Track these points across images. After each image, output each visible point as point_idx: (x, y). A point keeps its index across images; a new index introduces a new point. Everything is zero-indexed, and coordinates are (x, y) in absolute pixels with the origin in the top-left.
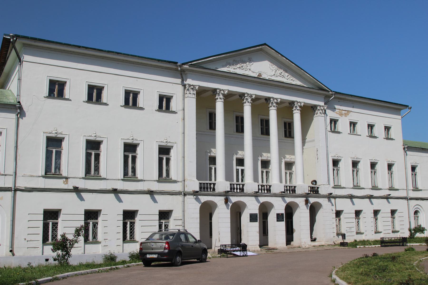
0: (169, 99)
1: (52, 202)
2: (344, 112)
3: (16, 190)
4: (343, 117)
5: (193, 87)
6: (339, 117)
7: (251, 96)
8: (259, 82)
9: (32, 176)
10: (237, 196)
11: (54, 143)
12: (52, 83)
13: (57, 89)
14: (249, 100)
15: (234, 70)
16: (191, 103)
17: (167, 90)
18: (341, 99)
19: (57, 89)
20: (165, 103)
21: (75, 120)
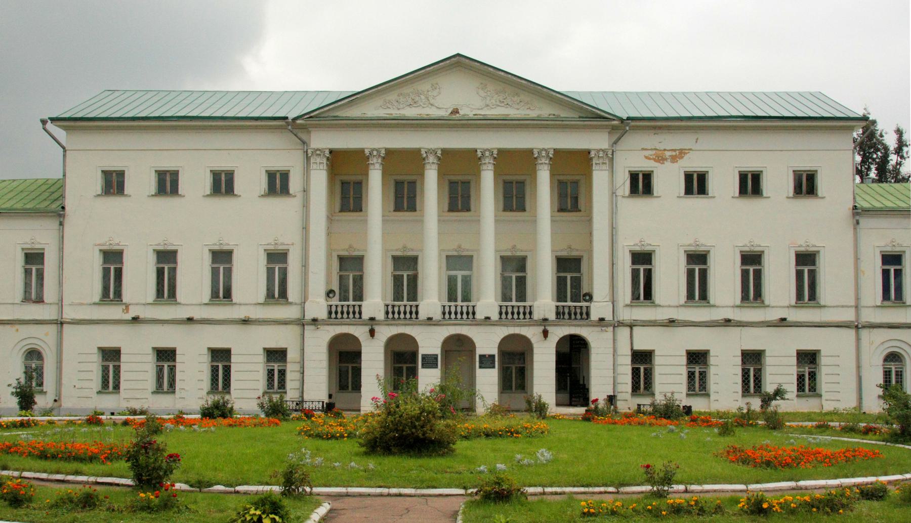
0: (285, 176)
1: (111, 338)
2: (668, 154)
3: (62, 323)
4: (668, 164)
5: (318, 152)
6: (657, 164)
7: (434, 152)
8: (454, 122)
9: (81, 304)
10: (397, 325)
11: (113, 258)
12: (107, 174)
13: (114, 183)
14: (432, 159)
15: (398, 112)
16: (320, 178)
17: (278, 163)
18: (660, 128)
19: (114, 183)
20: (277, 184)
21: (139, 225)
